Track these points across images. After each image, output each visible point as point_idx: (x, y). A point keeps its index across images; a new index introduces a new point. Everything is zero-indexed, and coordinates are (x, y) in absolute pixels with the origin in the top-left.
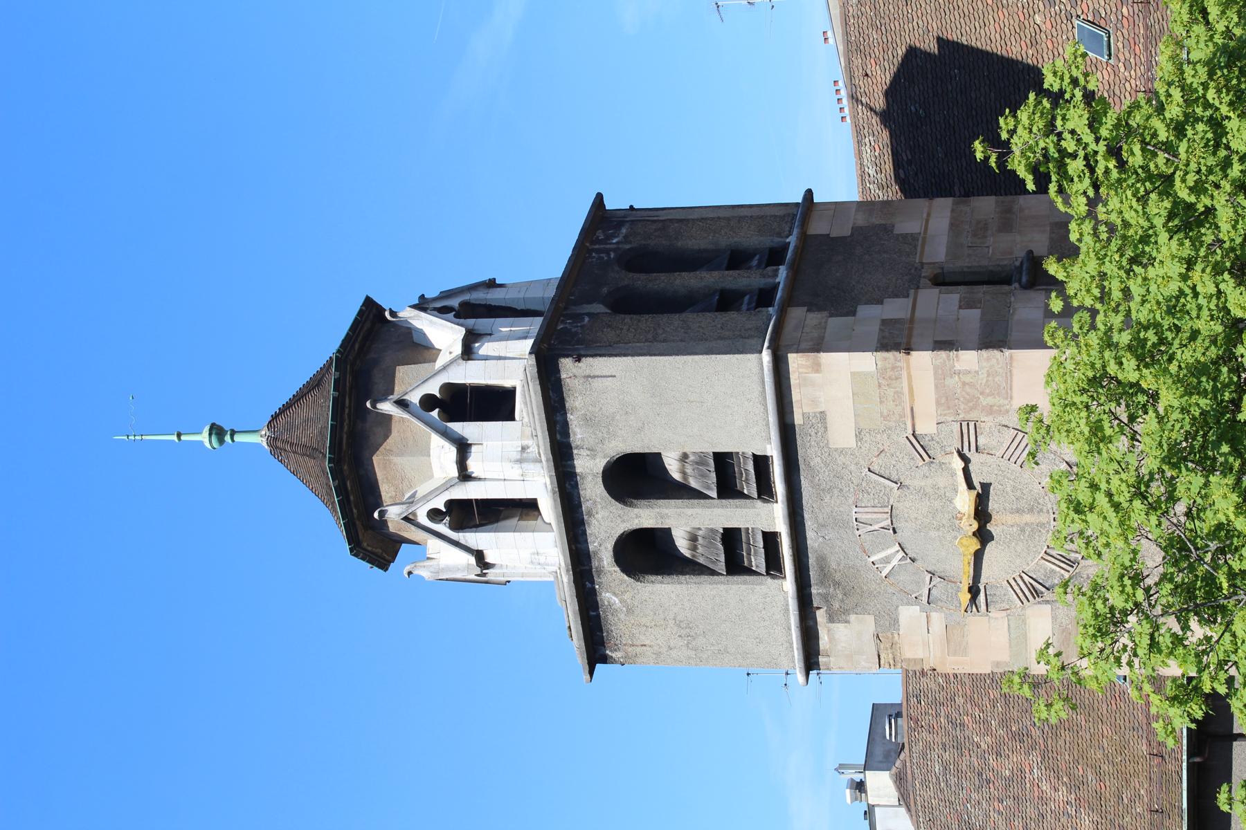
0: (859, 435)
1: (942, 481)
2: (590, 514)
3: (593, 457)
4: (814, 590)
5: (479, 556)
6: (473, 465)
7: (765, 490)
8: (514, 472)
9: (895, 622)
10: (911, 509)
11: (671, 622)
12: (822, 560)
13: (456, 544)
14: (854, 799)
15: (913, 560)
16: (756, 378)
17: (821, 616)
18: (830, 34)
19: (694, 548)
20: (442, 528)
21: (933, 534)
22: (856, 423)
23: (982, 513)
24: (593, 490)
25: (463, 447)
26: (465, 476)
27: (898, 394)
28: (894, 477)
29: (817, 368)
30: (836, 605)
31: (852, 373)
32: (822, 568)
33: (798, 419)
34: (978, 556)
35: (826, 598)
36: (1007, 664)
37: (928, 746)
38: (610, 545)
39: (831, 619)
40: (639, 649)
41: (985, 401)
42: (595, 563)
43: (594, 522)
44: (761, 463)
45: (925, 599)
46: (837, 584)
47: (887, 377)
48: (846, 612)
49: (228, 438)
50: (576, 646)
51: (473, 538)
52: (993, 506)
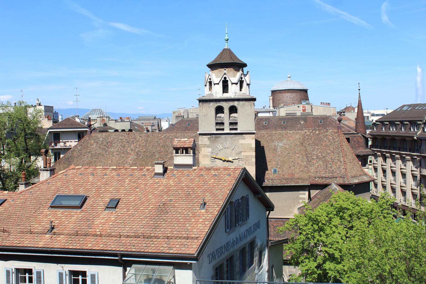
0: (241, 144)
1: (233, 155)
2: (227, 103)
3: (237, 104)
4: (214, 136)
5: (218, 84)
6: (234, 85)
7: (231, 129)
8: (233, 91)
9: (208, 147)
10: (229, 151)
11: (207, 113)
12: (220, 137)
13: (220, 81)
14: (37, 104)
15: (220, 151)
16: (251, 130)
17: (209, 136)
18: (194, 107)
19: (219, 117)
20: (223, 79)
21: (224, 154)
22: (243, 144)
23: (228, 161)
24: (231, 104)
25: (236, 84)
26: (232, 84)
27: (248, 150)
28: (234, 149)
29: (253, 139)
30: (211, 139)
31: (251, 144)
32: (218, 137)
33: (244, 135)
34: (221, 160)
35: (213, 137)
36: (201, 164)
37: (124, 136)
38: (221, 105)
39: (208, 138)
40: (202, 108)
41: (247, 162)
42: (218, 102)
43: (226, 103)
44: (236, 129)
45: (213, 152)
46: (215, 139)
47: (251, 149)
48: (210, 140)
49: (226, 41)
50: (200, 97)
51: (221, 84)
52: (229, 163)
